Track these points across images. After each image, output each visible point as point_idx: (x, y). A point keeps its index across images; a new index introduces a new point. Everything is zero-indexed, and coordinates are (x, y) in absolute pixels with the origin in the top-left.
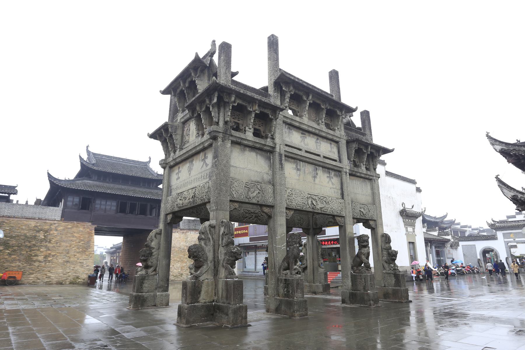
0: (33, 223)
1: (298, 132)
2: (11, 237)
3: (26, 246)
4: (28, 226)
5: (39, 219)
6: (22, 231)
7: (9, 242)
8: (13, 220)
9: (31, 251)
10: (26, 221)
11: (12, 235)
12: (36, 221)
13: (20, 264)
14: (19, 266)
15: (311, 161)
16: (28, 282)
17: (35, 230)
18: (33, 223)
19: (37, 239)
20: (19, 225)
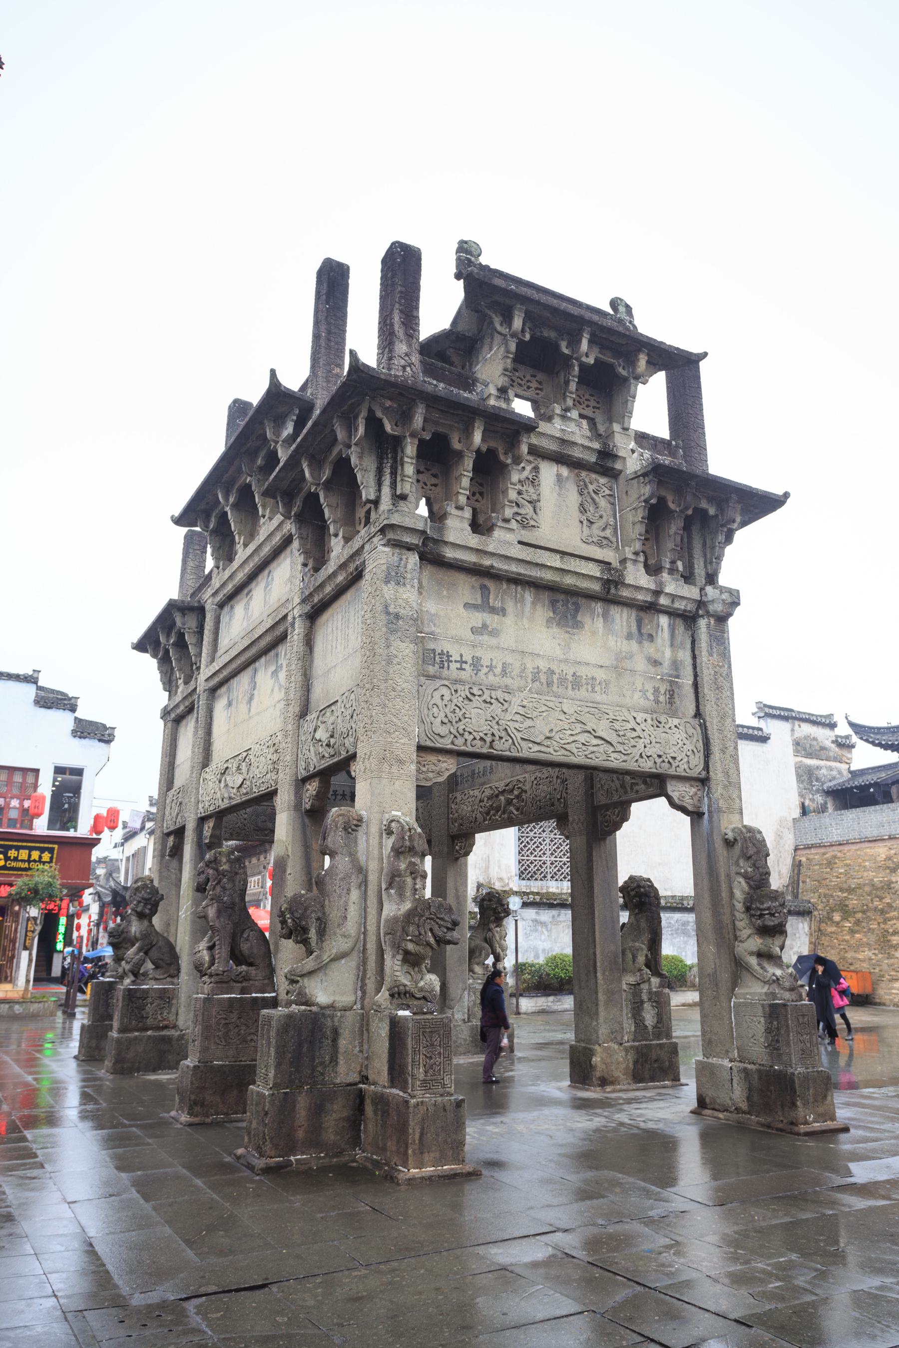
0: (881, 851)
1: (242, 599)
2: (850, 890)
3: (876, 909)
4: (873, 859)
5: (890, 838)
6: (865, 874)
7: (847, 902)
8: (849, 851)
9: (885, 922)
10: (871, 848)
11: (850, 887)
12: (888, 843)
13: (870, 954)
14: (871, 959)
15: (239, 662)
16: (891, 1000)
17: (888, 868)
18: (881, 851)
19: (893, 891)
20: (860, 860)
